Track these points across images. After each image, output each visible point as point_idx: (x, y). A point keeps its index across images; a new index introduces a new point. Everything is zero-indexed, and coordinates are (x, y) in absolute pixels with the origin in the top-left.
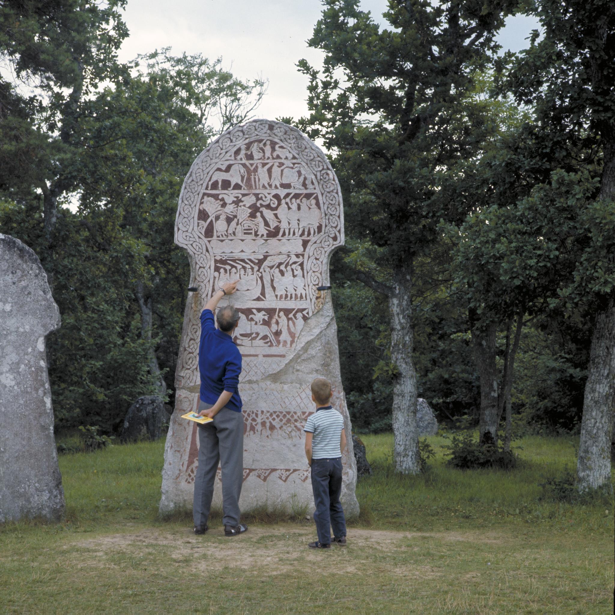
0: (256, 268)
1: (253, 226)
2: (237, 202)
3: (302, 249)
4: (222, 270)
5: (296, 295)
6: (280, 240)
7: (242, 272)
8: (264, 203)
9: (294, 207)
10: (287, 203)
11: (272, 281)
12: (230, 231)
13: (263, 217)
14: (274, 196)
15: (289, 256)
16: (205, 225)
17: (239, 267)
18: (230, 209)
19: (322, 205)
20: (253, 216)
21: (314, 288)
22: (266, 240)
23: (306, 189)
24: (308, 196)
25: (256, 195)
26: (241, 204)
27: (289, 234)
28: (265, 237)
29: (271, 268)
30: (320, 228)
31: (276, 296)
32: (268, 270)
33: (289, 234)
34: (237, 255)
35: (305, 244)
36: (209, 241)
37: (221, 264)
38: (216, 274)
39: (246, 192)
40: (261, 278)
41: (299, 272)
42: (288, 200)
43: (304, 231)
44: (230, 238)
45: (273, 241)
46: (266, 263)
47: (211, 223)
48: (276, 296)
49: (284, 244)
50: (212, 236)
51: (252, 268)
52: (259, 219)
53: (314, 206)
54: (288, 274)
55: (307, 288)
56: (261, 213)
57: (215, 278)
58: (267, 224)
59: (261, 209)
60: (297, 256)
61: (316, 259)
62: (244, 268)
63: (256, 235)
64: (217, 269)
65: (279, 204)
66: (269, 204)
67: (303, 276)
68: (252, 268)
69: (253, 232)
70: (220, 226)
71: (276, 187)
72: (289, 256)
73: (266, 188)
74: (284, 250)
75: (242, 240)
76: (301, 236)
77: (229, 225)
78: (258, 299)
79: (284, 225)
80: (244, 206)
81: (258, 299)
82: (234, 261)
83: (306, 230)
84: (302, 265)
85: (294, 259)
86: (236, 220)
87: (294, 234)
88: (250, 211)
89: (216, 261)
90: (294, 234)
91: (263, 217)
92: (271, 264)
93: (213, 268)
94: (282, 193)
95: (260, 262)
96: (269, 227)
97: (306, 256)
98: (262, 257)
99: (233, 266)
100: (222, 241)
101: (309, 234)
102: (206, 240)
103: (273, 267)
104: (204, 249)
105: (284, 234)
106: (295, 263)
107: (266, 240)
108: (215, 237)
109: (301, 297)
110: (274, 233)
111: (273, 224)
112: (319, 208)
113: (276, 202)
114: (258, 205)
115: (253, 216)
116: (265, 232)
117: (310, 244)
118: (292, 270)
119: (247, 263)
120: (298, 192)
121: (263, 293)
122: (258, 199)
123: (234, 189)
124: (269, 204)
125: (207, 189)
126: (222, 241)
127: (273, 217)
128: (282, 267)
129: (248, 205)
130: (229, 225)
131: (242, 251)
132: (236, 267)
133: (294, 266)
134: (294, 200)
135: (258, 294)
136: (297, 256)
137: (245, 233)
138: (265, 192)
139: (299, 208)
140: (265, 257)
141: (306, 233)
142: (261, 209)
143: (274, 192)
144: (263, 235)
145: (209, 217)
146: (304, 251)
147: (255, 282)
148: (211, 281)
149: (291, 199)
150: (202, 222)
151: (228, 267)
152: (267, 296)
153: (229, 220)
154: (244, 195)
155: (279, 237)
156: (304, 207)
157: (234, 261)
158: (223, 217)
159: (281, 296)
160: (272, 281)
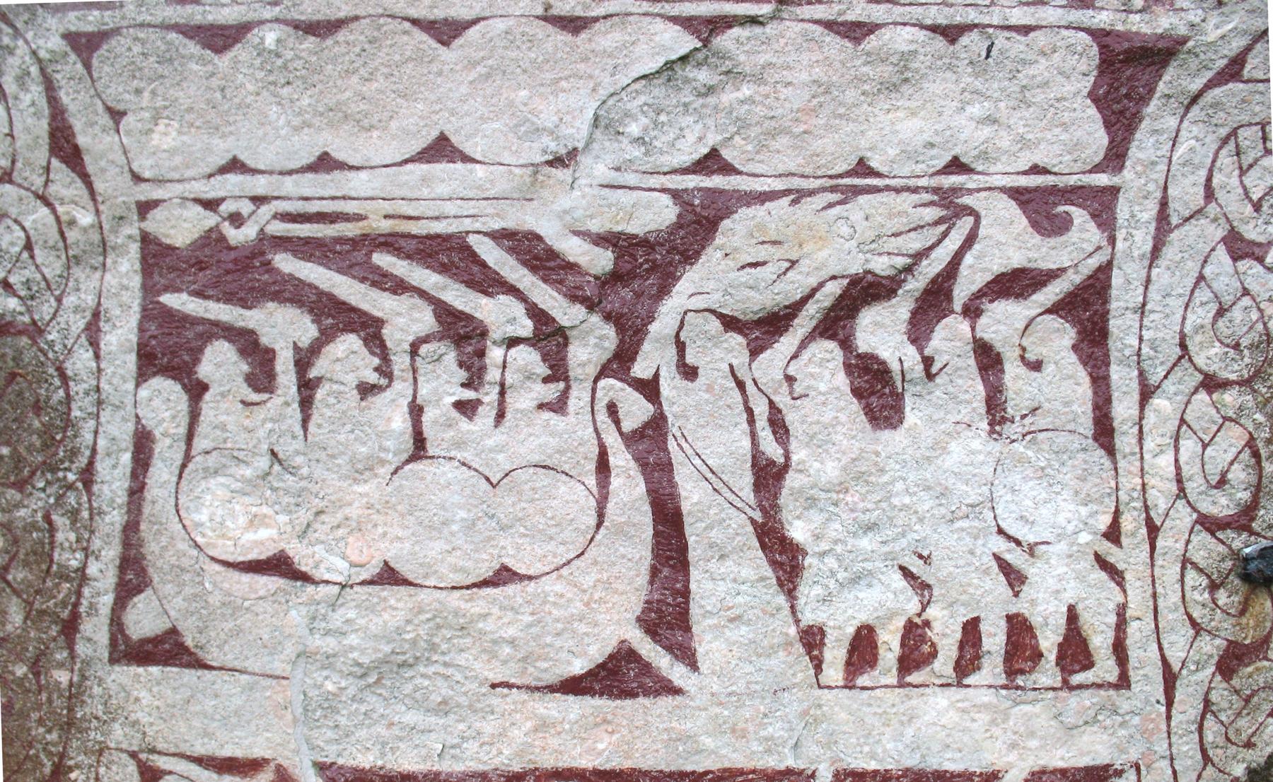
0: (592, 341)
3: (1097, 139)
4: (220, 364)
5: (1019, 629)
7: (442, 381)
11: (768, 476)
15: (951, 206)
17: (406, 320)
21: (1205, 548)
29: (765, 328)
31: (812, 639)
32: (721, 353)
34: (382, 188)
37: (216, 289)
38: (162, 401)
40: (651, 441)
41: (1061, 385)
46: (702, 285)
48: (812, 639)
49: (901, 78)
51: (549, 338)
54: (943, 416)
55: (1130, 556)
57: (143, 444)
60: (1042, 205)
61: (1238, 247)
62: (462, 333)
64: (168, 352)
67: (1104, 432)
68: (549, 338)
72: (951, 206)
74: (903, 133)
78: (616, 676)
81: (616, 676)
82: (352, 253)
84: (1087, 308)
85: (1007, 241)
89: (155, 255)
92: (755, 299)
93: (122, 335)
95: (641, 270)
97: (1134, 215)
98: (654, 215)
99: (336, 317)
103: (773, 324)
106: (1015, 283)
109: (1075, 651)
118: (988, 358)
119: (489, 283)
121: (669, 617)
128: (882, 332)
131: (441, 149)
132: (371, 330)
133: (1002, 322)
135: (616, 624)
136: (1042, 205)
140: (699, 224)
146: (1115, 157)
147: (576, 498)
148: (113, 479)
151: (284, 327)
152: (709, 641)
157: (352, 253)
159: (863, 648)
160: (768, 476)
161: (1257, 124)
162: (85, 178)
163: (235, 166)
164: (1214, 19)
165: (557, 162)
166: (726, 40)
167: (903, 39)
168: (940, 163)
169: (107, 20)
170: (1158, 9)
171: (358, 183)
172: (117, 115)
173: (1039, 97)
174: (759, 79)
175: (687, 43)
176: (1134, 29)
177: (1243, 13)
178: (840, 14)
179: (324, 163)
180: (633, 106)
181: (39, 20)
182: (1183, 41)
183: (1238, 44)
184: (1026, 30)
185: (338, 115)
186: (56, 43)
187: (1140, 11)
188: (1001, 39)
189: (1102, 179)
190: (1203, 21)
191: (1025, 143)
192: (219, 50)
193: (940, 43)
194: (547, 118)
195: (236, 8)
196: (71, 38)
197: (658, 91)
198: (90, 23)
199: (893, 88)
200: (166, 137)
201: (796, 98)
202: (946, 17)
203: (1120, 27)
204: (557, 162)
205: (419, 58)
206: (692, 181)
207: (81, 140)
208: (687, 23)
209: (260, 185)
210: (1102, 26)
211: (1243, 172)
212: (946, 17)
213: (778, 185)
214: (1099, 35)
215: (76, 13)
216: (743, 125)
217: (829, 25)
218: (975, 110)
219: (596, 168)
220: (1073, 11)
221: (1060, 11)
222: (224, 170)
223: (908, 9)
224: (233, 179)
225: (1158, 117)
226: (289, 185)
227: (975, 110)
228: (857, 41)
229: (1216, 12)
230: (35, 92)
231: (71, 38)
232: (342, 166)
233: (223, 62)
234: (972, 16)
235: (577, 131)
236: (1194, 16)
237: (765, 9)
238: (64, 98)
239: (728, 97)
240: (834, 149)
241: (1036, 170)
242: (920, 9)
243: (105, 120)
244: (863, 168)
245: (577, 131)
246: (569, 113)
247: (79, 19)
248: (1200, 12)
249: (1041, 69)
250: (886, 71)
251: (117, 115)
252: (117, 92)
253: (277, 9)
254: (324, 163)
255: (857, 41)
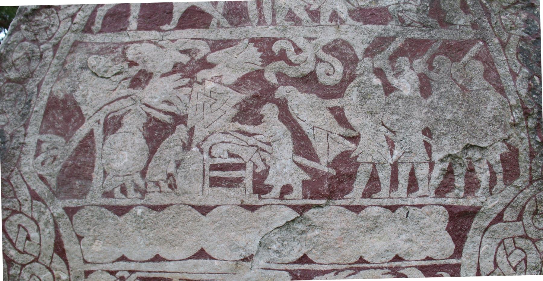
1: (246, 155)
2: (190, 69)
6: (357, 209)
8: (292, 73)
9: (406, 84)
10: (379, 72)
12: (157, 173)
13: (286, 116)
14: (330, 49)
16: (65, 148)
18: (159, 92)
19: (508, 83)
20: (248, 113)
22: (302, 209)
23: (445, 23)
24: (455, 50)
25: (264, 44)
26: (201, 75)
27: (394, 181)
28: (297, 196)
30: (510, 163)
33: (394, 181)
35: (460, 222)
36: (70, 212)
39: (224, 34)
42: (381, 61)
43: (449, 172)
44: (155, 198)
45: (331, 217)
47: (87, 145)
49: (375, 225)
50: (83, 194)
52: (272, 125)
53: (479, 83)
56: (283, 106)
58: (302, 144)
59: (281, 92)
63: (260, 188)
65: (349, 78)
66: (313, 74)
69: (247, 175)
70: (122, 155)
71: (334, 16)
73: (297, 21)
75: (205, 210)
76: (442, 190)
77: (152, 152)
79: (371, 149)
80: (218, 80)
83: (459, 170)
86: (181, 131)
87: (413, 184)
88: (236, 97)
90: (413, 184)
91: (286, 116)
94: (358, 37)
96: (313, 156)
100: (121, 211)
101: (472, 186)
102: (58, 207)
104: (49, 241)
105: (373, 187)
107: (302, 209)
108: (95, 196)
110: (332, 184)
111: (328, 147)
112: (501, 90)
113: (339, 68)
114: (270, 77)
115: (248, 113)
116: (296, 178)
117: (478, 222)
120: (417, 35)
122: (269, 58)
123: (181, 26)
124: (313, 74)
125: (88, 29)
126: (121, 211)
127: (326, 120)
129: (232, 77)
130: (152, 152)
131: (201, 254)
134: (403, 61)
137: (215, 182)
138: (298, 35)
139: (425, 87)
141: (460, 182)
142: (281, 92)
143: (329, 35)
144: (287, 190)
145: (82, 119)
146: (458, 252)
149: (392, 58)
150: (49, 138)
153: (156, 132)
154: (217, 45)
155: (355, 196)
156: (442, 88)
158: (133, 124)
161: (511, 238)
162: (66, 261)
163: (123, 258)
164: (490, 200)
165: (245, 259)
166: (309, 214)
167: (375, 211)
168: (391, 258)
169: (80, 203)
170: (469, 197)
171: (170, 266)
172: (80, 238)
173: (427, 231)
174: (321, 228)
175: (294, 215)
176: (461, 204)
177: (500, 197)
178: (351, 203)
179: (157, 259)
180: (274, 238)
181: (55, 202)
182: (480, 208)
183: (500, 208)
184: (420, 206)
185: (163, 241)
186: (60, 211)
187: (462, 198)
188: (411, 210)
189: (454, 261)
190: (486, 200)
191: (423, 248)
192: (120, 215)
193: (389, 212)
194: (242, 243)
195: (127, 200)
196: (66, 209)
197: (284, 233)
198: (74, 204)
199: (372, 230)
200: (98, 247)
201: (336, 234)
202: (391, 203)
203: (455, 204)
204: (245, 259)
205: (194, 220)
206: (297, 267)
207: (66, 247)
208: (294, 207)
209: (132, 266)
210: (449, 204)
211: (508, 256)
212: (391, 203)
213: (330, 268)
214: (448, 207)
215: (69, 200)
216: (315, 245)
217: (347, 207)
218: (404, 237)
219: (260, 262)
220: (438, 199)
221: (433, 199)
222: (119, 260)
223: (376, 200)
224: (122, 263)
225: (473, 238)
226: (143, 267)
227: (404, 237)
228: (358, 212)
229: (490, 197)
230: (51, 228)
231: (66, 209)
232: (164, 260)
233: (121, 219)
234: (400, 202)
235: (253, 248)
236: (483, 199)
237: (323, 202)
238: (61, 231)
239: (310, 235)
240: (351, 254)
241: (428, 258)
242: (381, 200)
243: (76, 240)
244: (362, 260)
245: (253, 248)
246: (250, 241)
247: (70, 202)
248: (484, 197)
249: (427, 220)
250: (369, 224)
251: (80, 238)
252: (81, 229)
253: (142, 201)
254: (157, 259)
255: (358, 212)
